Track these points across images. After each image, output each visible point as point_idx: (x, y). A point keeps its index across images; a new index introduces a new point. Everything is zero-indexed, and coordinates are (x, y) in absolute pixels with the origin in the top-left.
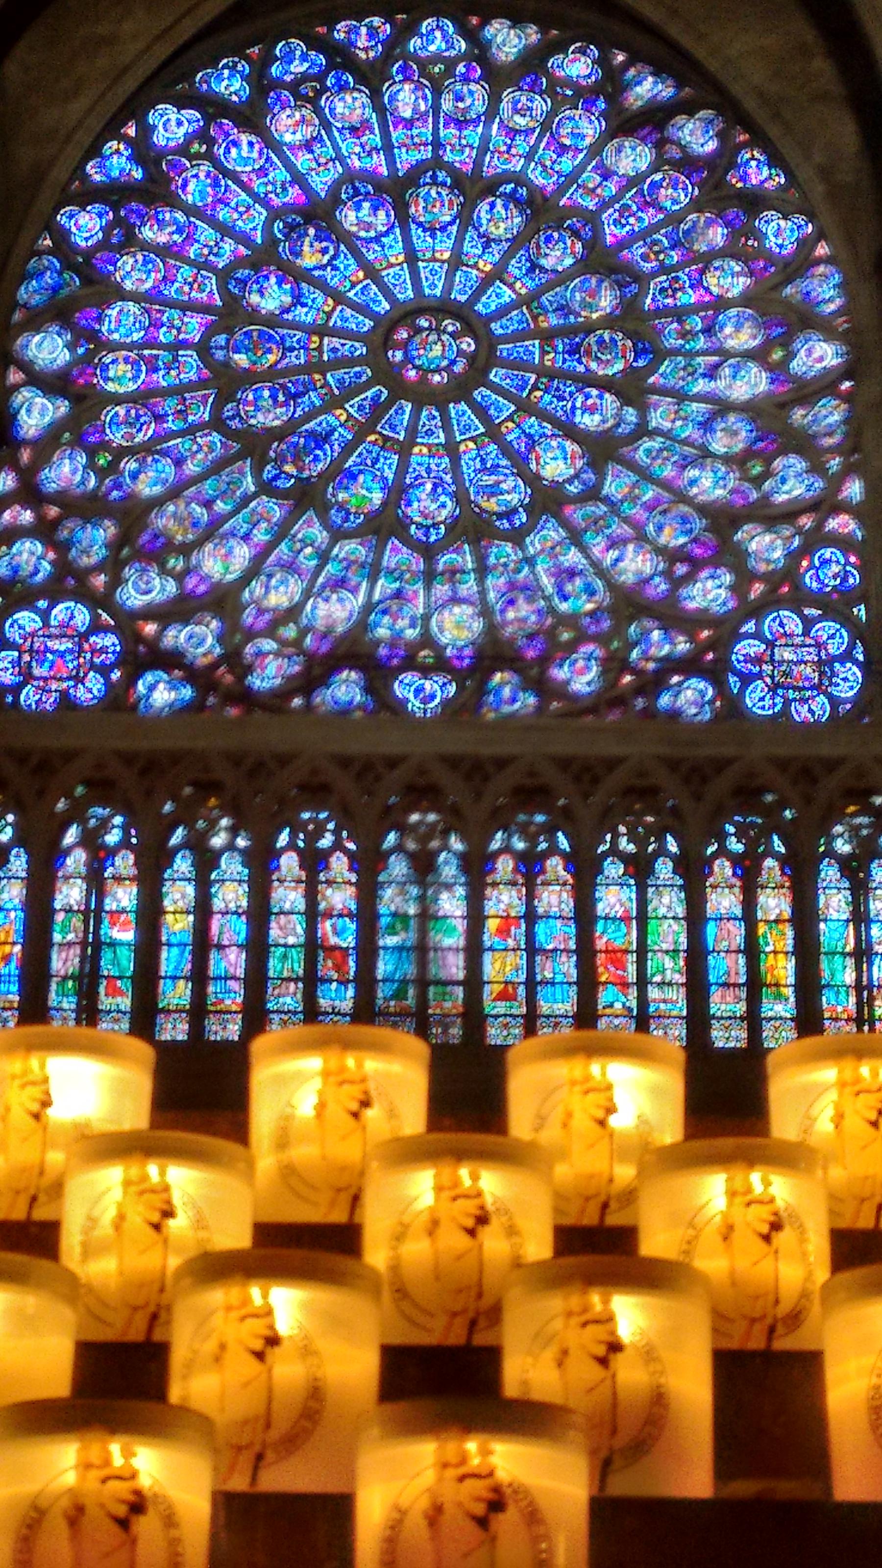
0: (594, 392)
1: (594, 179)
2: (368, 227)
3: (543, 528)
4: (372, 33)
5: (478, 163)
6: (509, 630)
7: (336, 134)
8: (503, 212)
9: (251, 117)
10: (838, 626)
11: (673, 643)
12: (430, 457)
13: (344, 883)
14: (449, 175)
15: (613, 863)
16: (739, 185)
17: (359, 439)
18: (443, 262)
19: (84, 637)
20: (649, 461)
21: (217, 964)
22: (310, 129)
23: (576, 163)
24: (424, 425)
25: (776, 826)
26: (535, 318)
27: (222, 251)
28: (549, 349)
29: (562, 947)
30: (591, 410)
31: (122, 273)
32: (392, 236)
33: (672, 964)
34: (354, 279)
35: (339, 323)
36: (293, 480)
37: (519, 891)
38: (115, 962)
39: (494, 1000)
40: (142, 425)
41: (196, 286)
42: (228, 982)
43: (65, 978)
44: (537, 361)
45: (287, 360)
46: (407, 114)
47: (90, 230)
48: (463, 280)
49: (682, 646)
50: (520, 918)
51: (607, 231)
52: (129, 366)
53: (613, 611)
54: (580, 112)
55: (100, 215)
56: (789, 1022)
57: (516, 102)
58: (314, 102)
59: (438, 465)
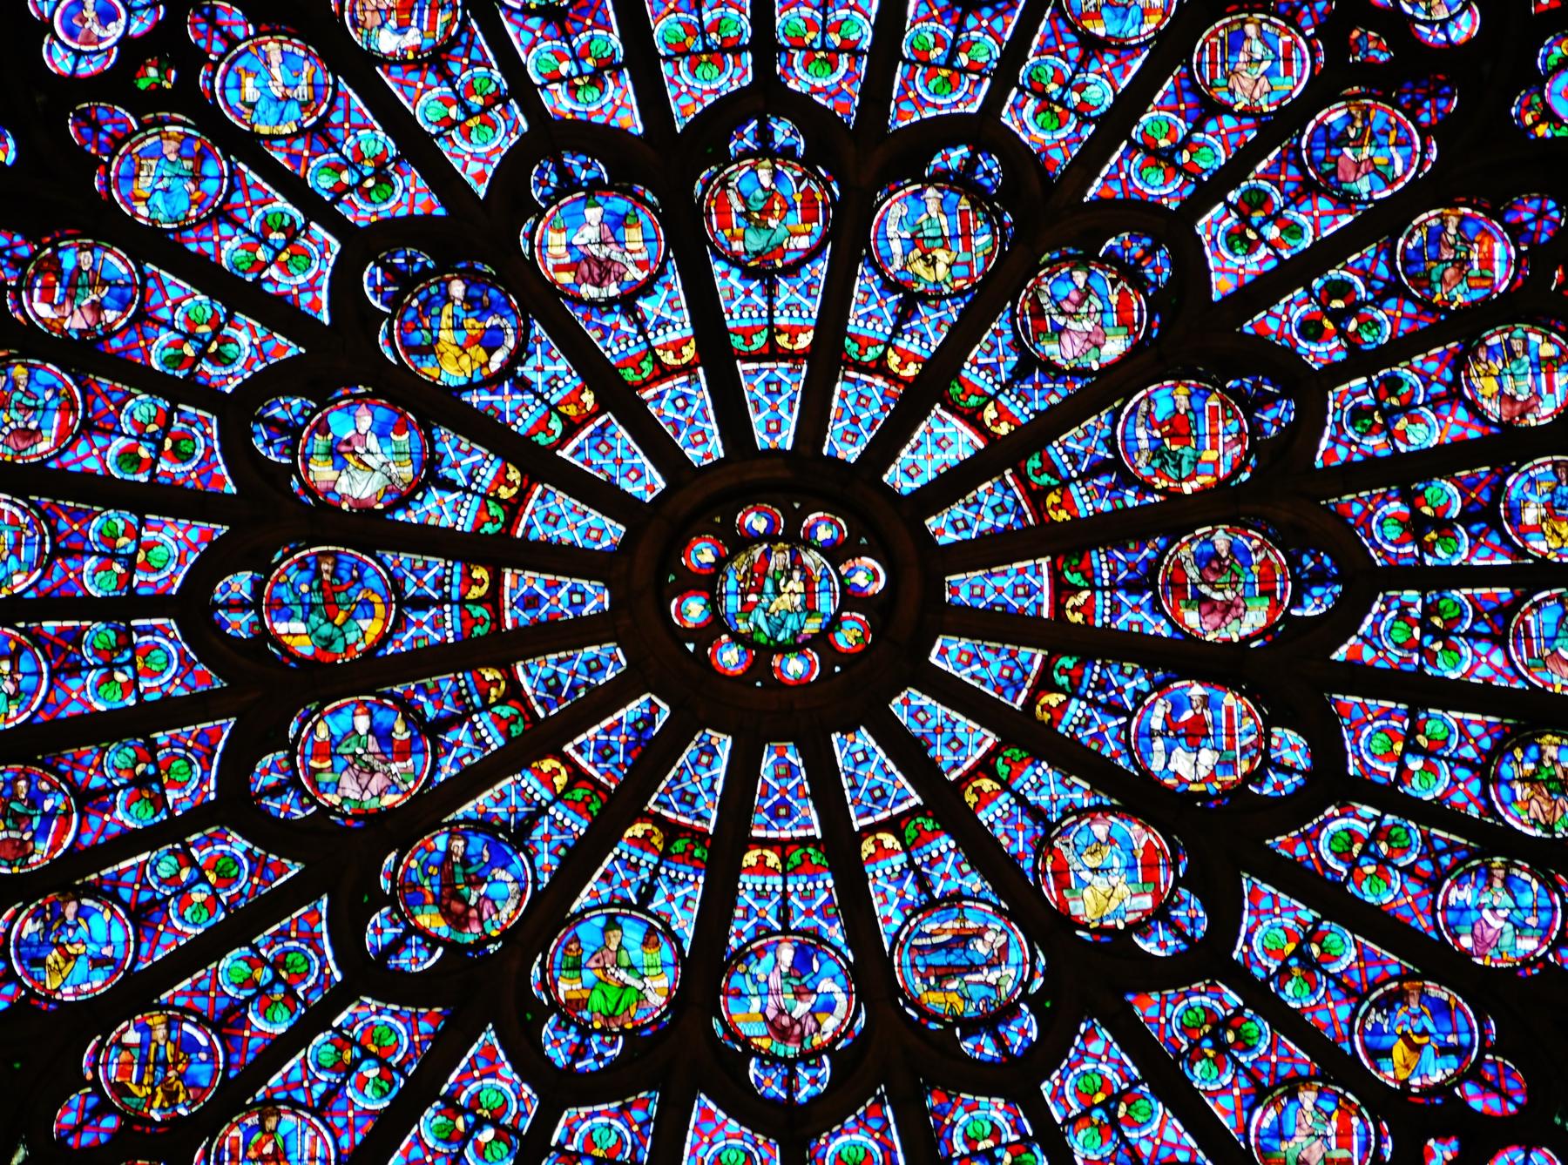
0: (1197, 690)
1: (1172, 128)
2: (603, 270)
3: (1083, 1054)
5: (876, 92)
7: (511, 29)
12: (785, 874)
14: (802, 127)
16: (1542, 130)
20: (1341, 868)
22: (443, 18)
23: (1123, 84)
26: (1037, 497)
27: (232, 347)
28: (1075, 579)
30: (1195, 734)
32: (663, 294)
34: (572, 411)
35: (538, 532)
36: (440, 951)
41: (168, 443)
44: (1045, 615)
45: (412, 631)
48: (850, 401)
51: (1213, 263)
59: (807, 897)
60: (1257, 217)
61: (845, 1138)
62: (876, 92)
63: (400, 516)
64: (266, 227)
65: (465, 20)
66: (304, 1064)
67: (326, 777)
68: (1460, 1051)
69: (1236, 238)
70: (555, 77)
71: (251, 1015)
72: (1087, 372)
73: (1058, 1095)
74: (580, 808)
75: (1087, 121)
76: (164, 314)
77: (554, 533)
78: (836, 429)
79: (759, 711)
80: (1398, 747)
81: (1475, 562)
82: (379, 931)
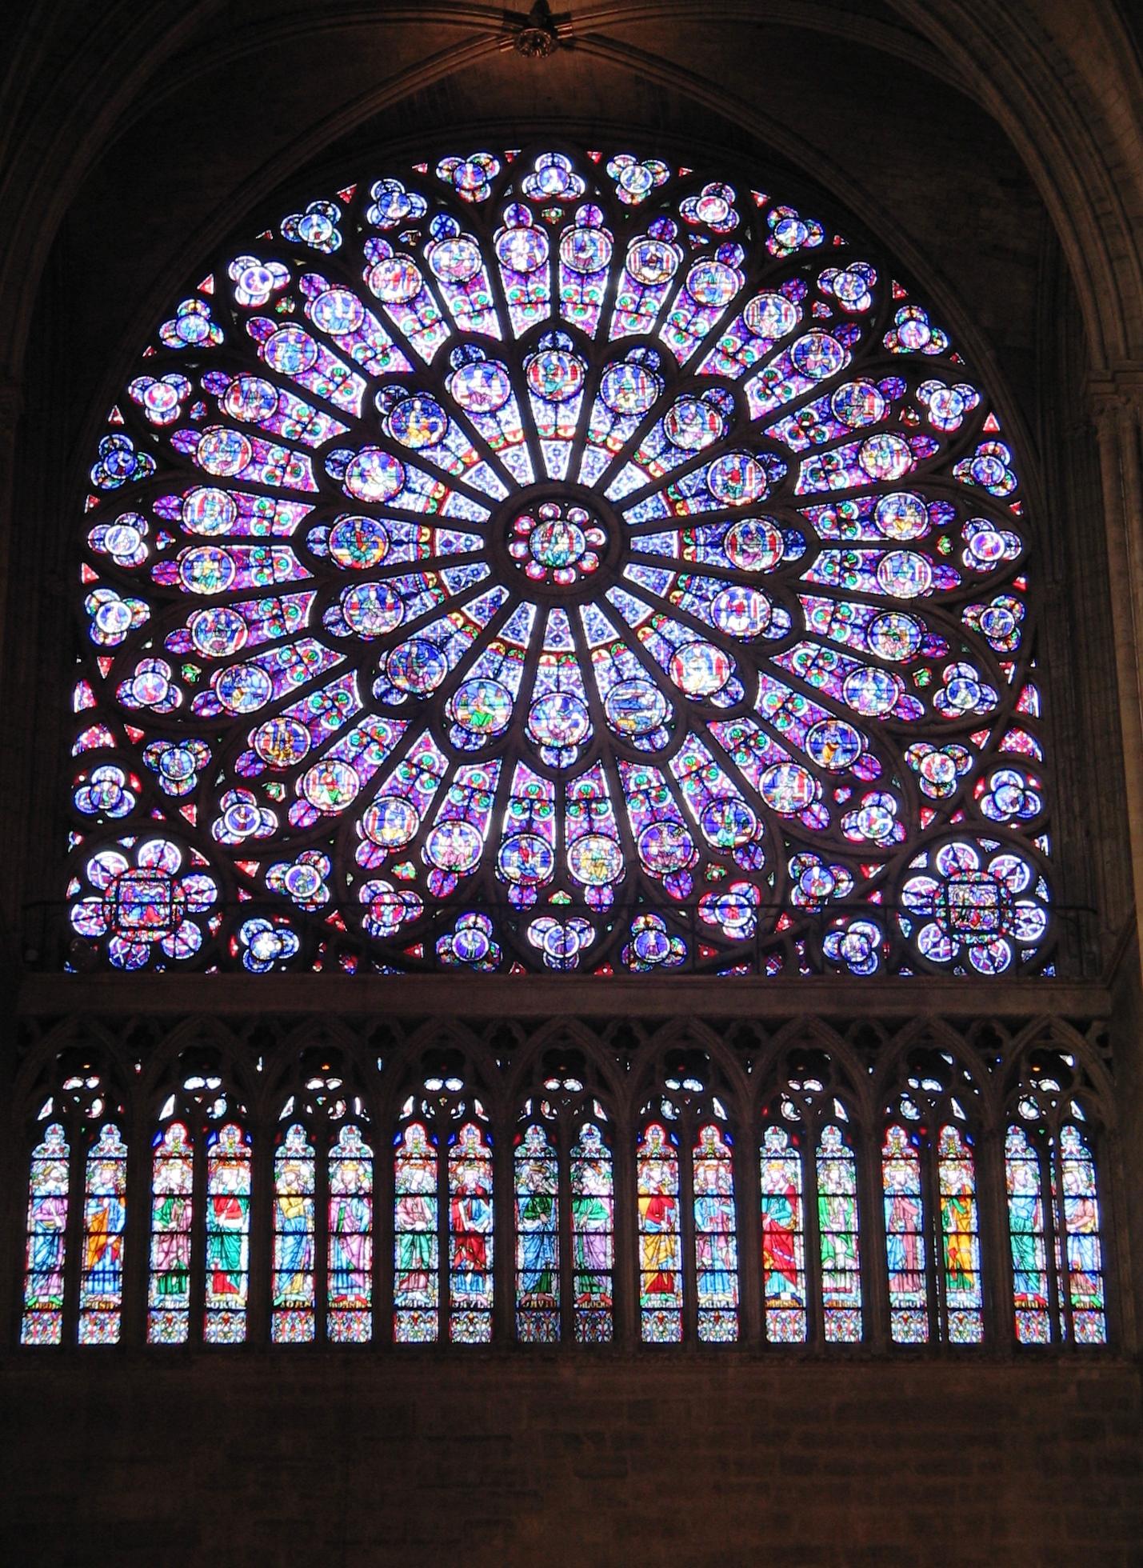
0: (740, 591)
2: (483, 398)
3: (688, 748)
4: (480, 169)
5: (604, 324)
7: (442, 289)
8: (633, 381)
9: (345, 269)
10: (1018, 860)
11: (837, 881)
13: (476, 1158)
15: (775, 1132)
16: (897, 350)
18: (566, 440)
19: (176, 879)
20: (803, 671)
21: (340, 1255)
22: (413, 284)
23: (715, 322)
28: (688, 541)
30: (739, 610)
31: (205, 454)
34: (467, 460)
35: (452, 513)
37: (672, 1167)
40: (234, 632)
42: (352, 1276)
43: (168, 1273)
44: (675, 555)
46: (521, 265)
47: (166, 404)
49: (846, 886)
51: (751, 403)
52: (216, 564)
53: (767, 844)
54: (715, 264)
55: (177, 387)
56: (975, 1314)
57: (643, 253)
58: (416, 254)
59: (568, 678)
60: (771, 384)
61: (582, 783)
62: (604, 324)
63: (391, 504)
64: (333, 375)
67: (356, 618)
68: (852, 751)
70: (462, 313)
72: (694, 450)
73: (676, 766)
74: (469, 635)
75: (697, 339)
76: (287, 411)
77: (459, 514)
78: (584, 471)
79: (548, 594)
80: (829, 619)
81: (864, 539)
82: (379, 686)
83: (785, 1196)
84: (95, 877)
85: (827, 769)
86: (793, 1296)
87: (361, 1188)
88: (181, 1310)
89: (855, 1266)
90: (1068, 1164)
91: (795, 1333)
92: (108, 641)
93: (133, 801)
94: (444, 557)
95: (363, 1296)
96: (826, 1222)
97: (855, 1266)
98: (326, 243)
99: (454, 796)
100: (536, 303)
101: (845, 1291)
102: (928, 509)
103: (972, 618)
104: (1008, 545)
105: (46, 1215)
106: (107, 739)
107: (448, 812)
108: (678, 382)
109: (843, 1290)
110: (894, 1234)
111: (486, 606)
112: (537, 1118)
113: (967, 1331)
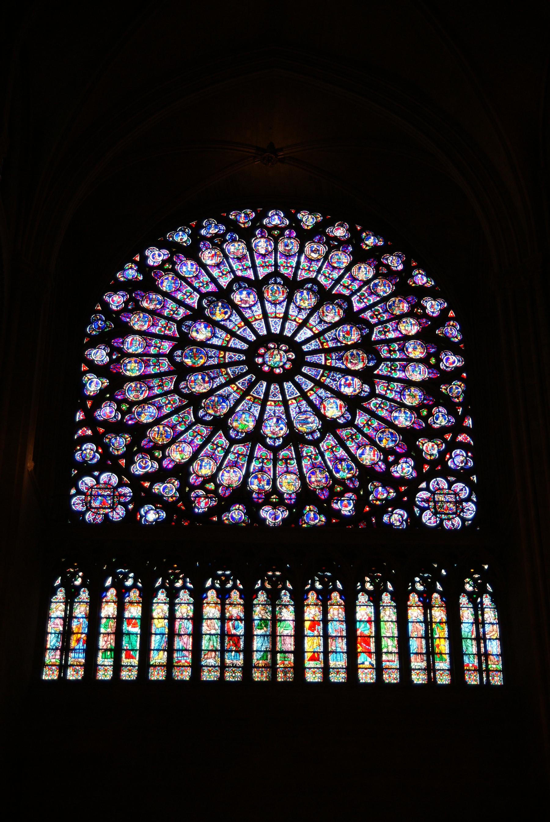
0: (350, 378)
2: (246, 302)
3: (327, 439)
4: (247, 216)
5: (295, 274)
6: (313, 486)
7: (231, 260)
8: (307, 296)
9: (192, 253)
11: (388, 493)
15: (363, 595)
16: (413, 285)
17: (242, 398)
18: (280, 318)
19: (115, 488)
20: (375, 409)
21: (178, 644)
22: (219, 258)
23: (340, 274)
24: (272, 393)
25: (437, 577)
29: (339, 635)
30: (349, 385)
31: (133, 322)
32: (257, 306)
33: (392, 643)
34: (240, 326)
35: (233, 346)
38: (130, 643)
39: (309, 660)
40: (143, 391)
41: (167, 328)
43: (106, 650)
44: (323, 363)
46: (263, 252)
47: (118, 303)
49: (393, 494)
50: (320, 621)
51: (354, 305)
52: (137, 365)
53: (359, 478)
54: (340, 252)
55: (123, 296)
57: (311, 248)
59: (279, 411)
62: (295, 274)
63: (208, 342)
65: (223, 259)
66: (187, 435)
67: (193, 386)
69: (359, 301)
70: (238, 269)
71: (178, 427)
73: (323, 446)
74: (238, 393)
76: (168, 306)
79: (271, 377)
80: (386, 389)
83: (367, 621)
84: (82, 487)
85: (385, 448)
86: (370, 663)
87: (188, 616)
88: (110, 666)
89: (396, 651)
90: (486, 610)
91: (371, 679)
92: (92, 394)
93: (99, 457)
94: (229, 362)
95: (188, 661)
96: (384, 632)
97: (396, 651)
98: (185, 242)
99: (231, 457)
100: (269, 266)
101: (392, 661)
102: (426, 347)
103: (444, 389)
104: (459, 361)
105: (55, 626)
106: (89, 432)
107: (228, 463)
108: (325, 296)
109: (391, 661)
110: (413, 638)
111: (246, 382)
112: (263, 588)
113: (444, 679)
